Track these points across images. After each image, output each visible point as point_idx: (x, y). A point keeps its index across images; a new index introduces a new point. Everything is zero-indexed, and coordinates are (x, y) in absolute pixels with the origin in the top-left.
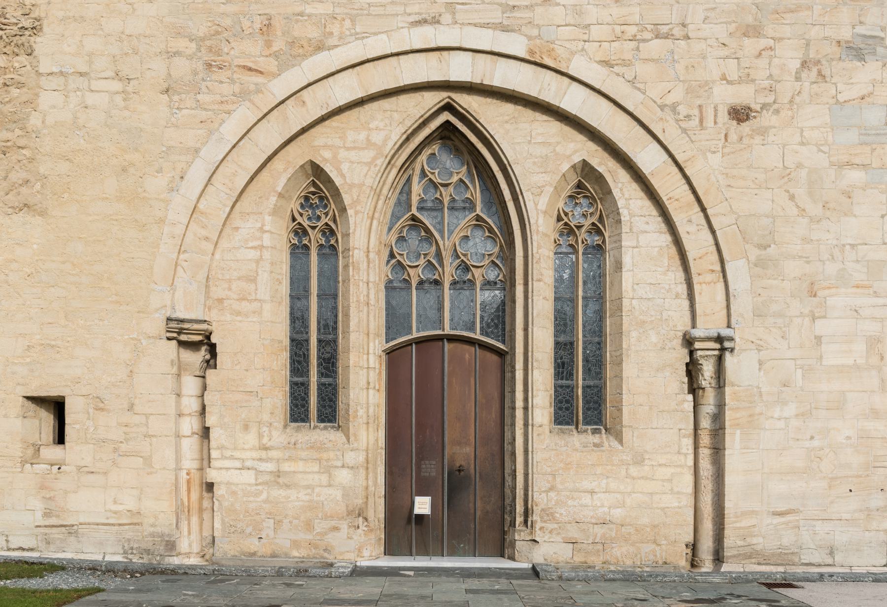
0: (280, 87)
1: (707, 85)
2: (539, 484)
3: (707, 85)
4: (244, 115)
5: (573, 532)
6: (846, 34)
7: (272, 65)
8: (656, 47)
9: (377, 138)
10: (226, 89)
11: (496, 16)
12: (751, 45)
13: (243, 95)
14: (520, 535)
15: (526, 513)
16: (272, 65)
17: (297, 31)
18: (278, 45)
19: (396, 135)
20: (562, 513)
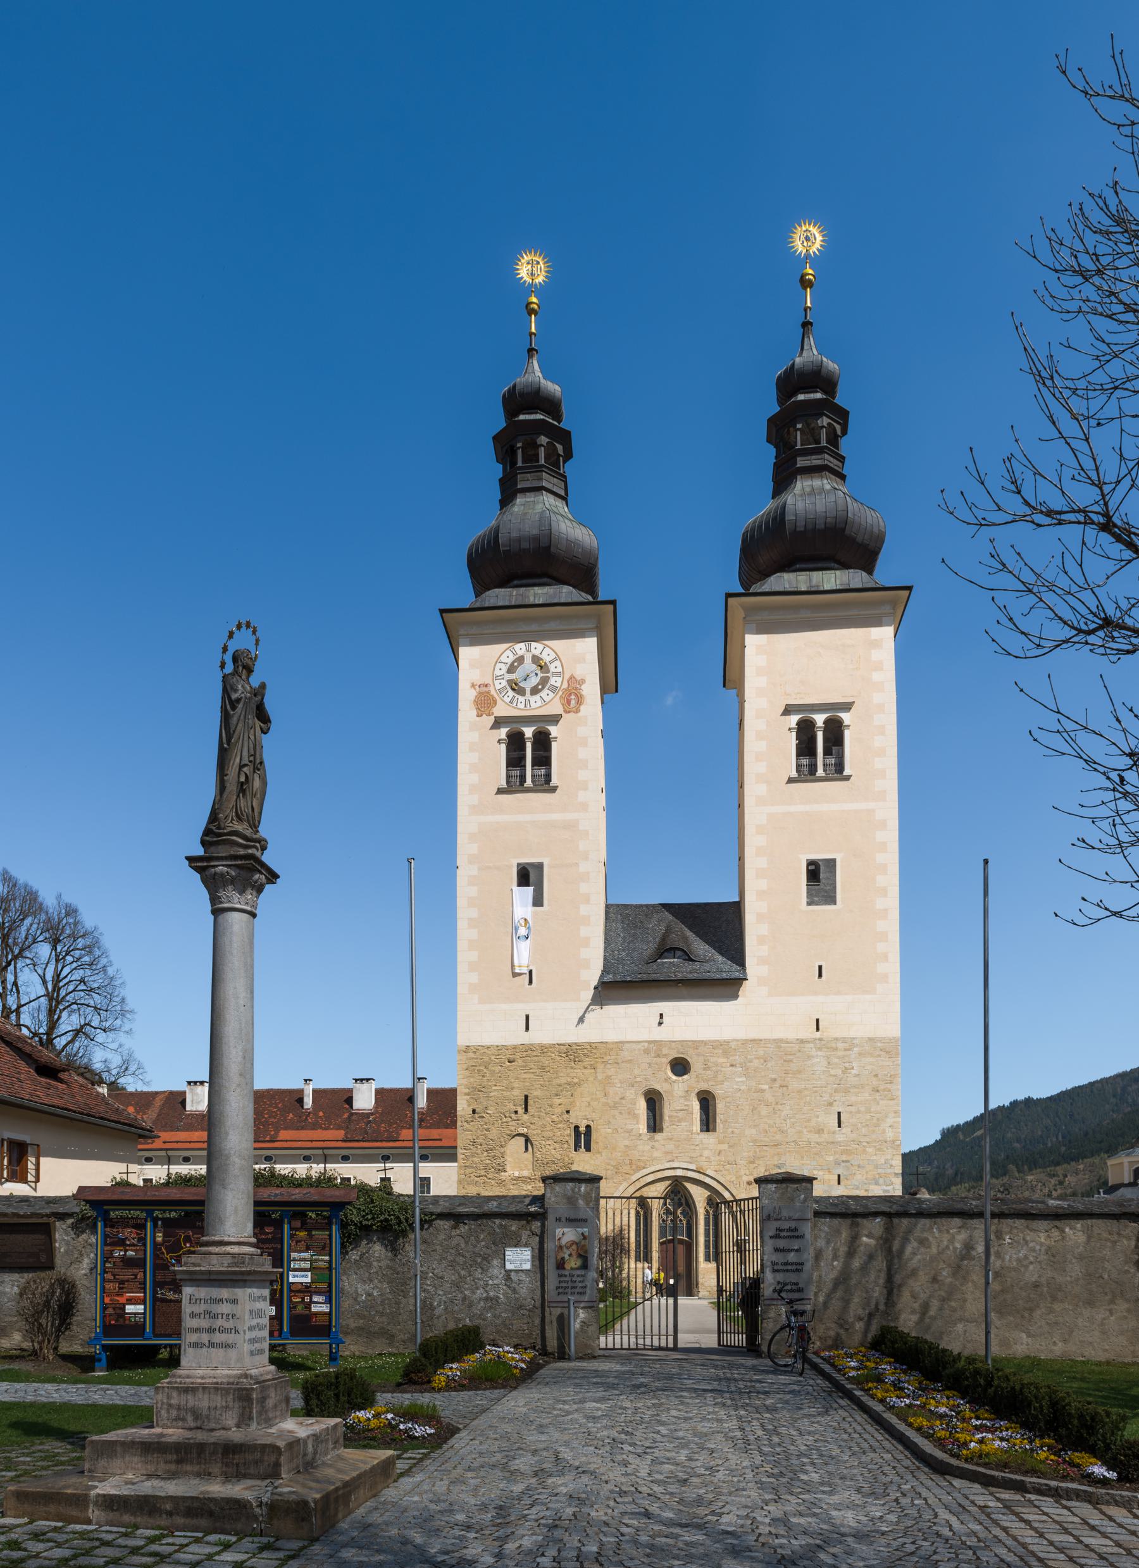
0: (634, 1178)
1: (741, 1176)
2: (700, 1276)
3: (741, 1176)
4: (625, 1185)
5: (709, 1289)
6: (776, 1163)
7: (632, 1172)
8: (728, 1167)
9: (658, 1189)
10: (621, 1178)
11: (689, 1160)
12: (752, 1166)
13: (625, 1180)
14: (695, 1290)
15: (697, 1284)
16: (632, 1172)
17: (638, 1163)
18: (634, 1167)
19: (663, 1189)
20: (706, 1284)
